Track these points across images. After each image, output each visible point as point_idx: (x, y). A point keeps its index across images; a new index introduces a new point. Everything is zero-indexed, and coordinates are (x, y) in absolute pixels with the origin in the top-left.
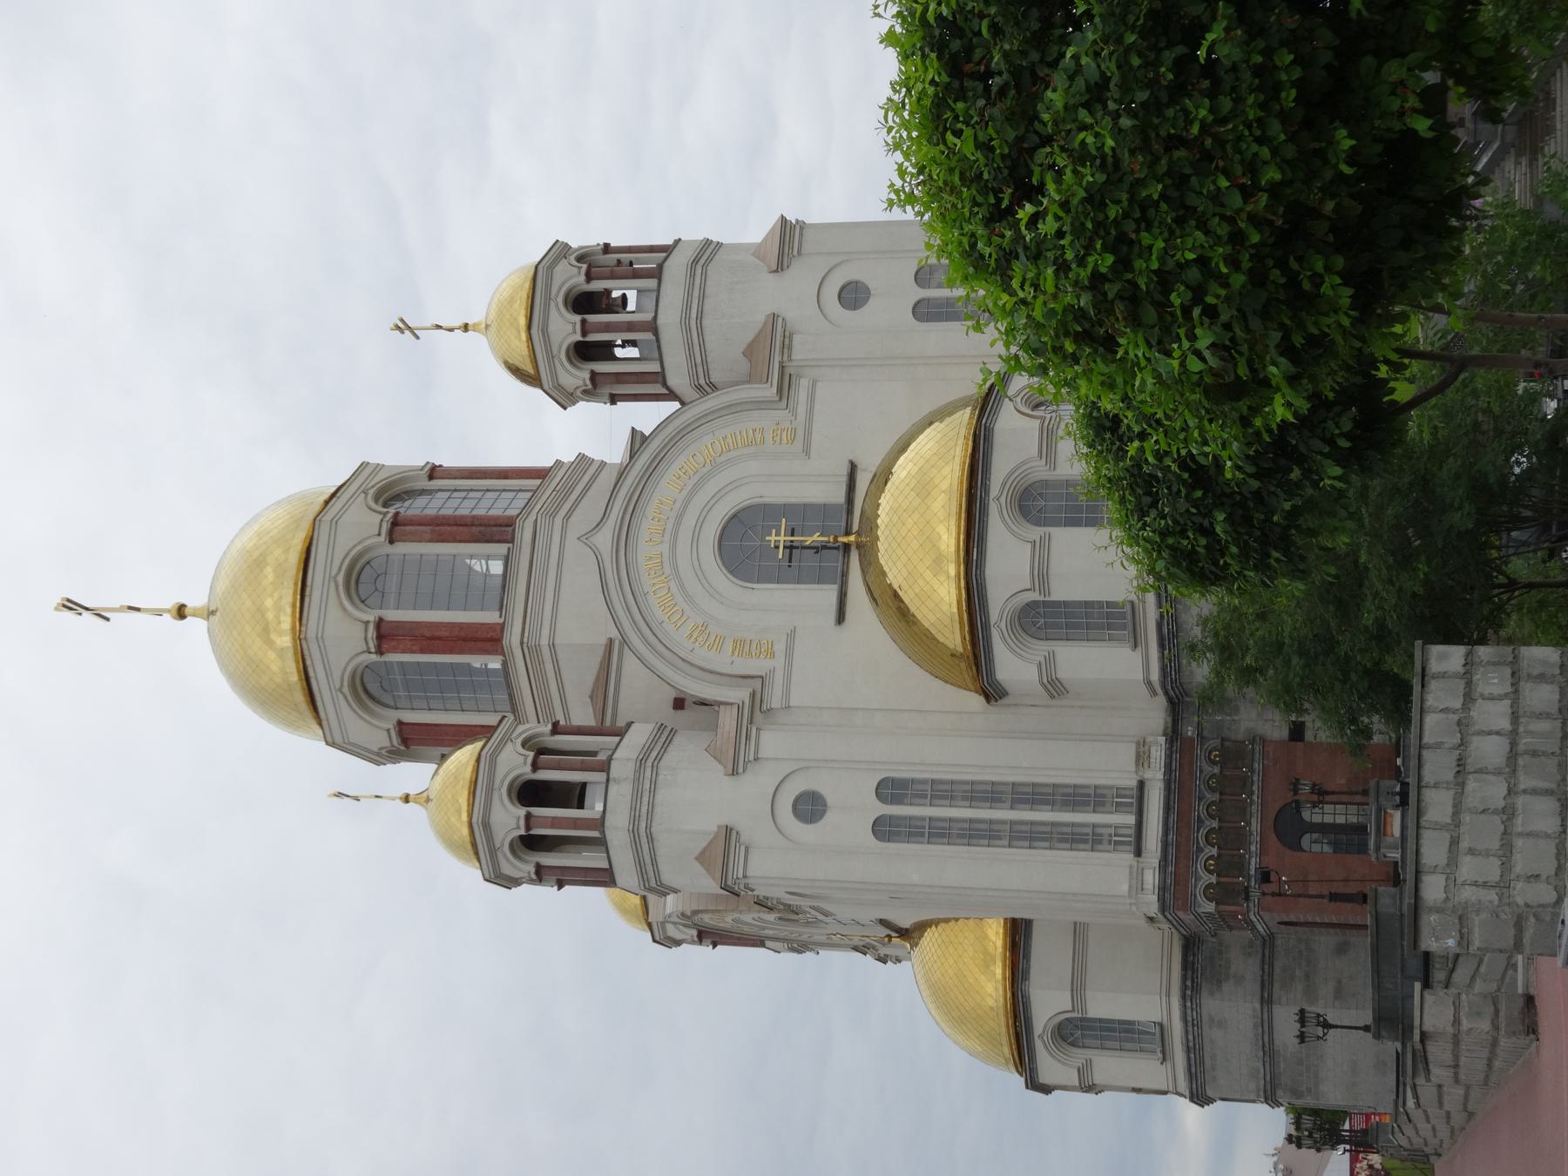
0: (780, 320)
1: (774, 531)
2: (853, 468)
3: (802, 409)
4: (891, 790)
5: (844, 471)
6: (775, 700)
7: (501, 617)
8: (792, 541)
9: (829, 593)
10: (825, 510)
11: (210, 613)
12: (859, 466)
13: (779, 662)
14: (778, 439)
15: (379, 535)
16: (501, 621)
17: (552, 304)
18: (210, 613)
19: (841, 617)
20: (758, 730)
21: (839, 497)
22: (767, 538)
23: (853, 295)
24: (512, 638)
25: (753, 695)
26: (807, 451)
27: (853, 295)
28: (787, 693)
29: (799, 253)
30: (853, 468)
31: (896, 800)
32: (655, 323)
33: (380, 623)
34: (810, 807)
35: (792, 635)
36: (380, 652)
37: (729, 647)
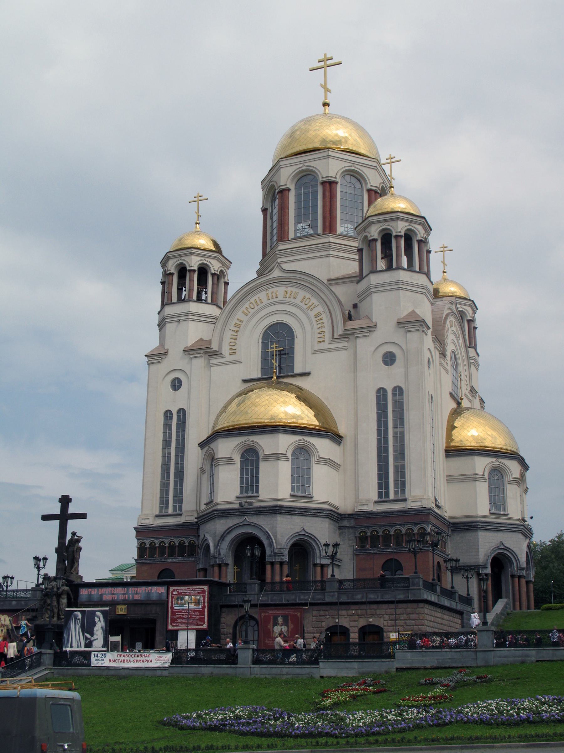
2: (307, 374)
4: (182, 413)
5: (307, 371)
6: (213, 361)
8: (276, 355)
9: (257, 374)
10: (292, 367)
15: (323, 178)
19: (245, 381)
21: (297, 370)
22: (275, 343)
25: (215, 351)
26: (316, 352)
30: (307, 374)
31: (178, 417)
33: (289, 190)
34: (176, 384)
35: (239, 362)
36: (278, 193)
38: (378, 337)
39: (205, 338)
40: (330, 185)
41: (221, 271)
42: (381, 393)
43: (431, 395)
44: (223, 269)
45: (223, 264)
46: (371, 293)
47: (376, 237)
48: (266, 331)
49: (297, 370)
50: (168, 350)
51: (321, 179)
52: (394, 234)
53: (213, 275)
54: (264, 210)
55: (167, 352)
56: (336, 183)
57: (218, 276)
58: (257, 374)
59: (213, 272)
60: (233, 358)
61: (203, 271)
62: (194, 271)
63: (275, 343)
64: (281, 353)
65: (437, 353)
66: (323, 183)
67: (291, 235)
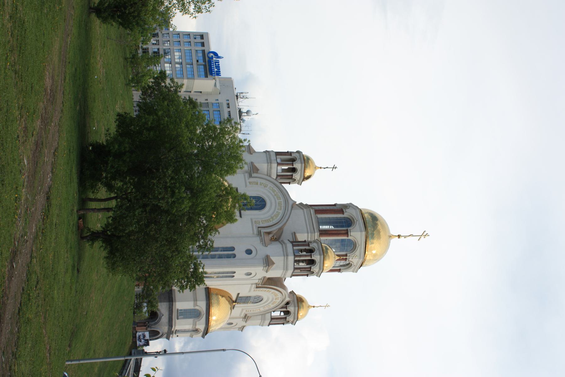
0: (264, 245)
3: (255, 228)
5: (242, 216)
6: (247, 175)
7: (317, 216)
11: (391, 237)
12: (239, 217)
13: (248, 181)
14: (259, 222)
15: (350, 230)
16: (316, 215)
17: (317, 248)
18: (391, 237)
20: (249, 170)
21: (242, 212)
23: (249, 252)
24: (312, 211)
25: (251, 175)
26: (251, 219)
27: (249, 252)
28: (244, 176)
29: (263, 259)
32: (294, 257)
33: (343, 214)
35: (246, 186)
37: (259, 184)
38: (260, 246)
39: (259, 172)
40: (347, 234)
41: (295, 180)
42: (233, 249)
43: (233, 276)
44: (297, 180)
45: (299, 181)
46: (282, 244)
47: (310, 245)
48: (261, 198)
50: (252, 154)
52: (312, 254)
53: (292, 175)
54: (335, 205)
55: (251, 154)
56: (348, 236)
57: (291, 177)
59: (294, 175)
60: (248, 184)
61: (294, 170)
62: (293, 165)
65: (257, 281)
66: (347, 230)
67: (320, 216)
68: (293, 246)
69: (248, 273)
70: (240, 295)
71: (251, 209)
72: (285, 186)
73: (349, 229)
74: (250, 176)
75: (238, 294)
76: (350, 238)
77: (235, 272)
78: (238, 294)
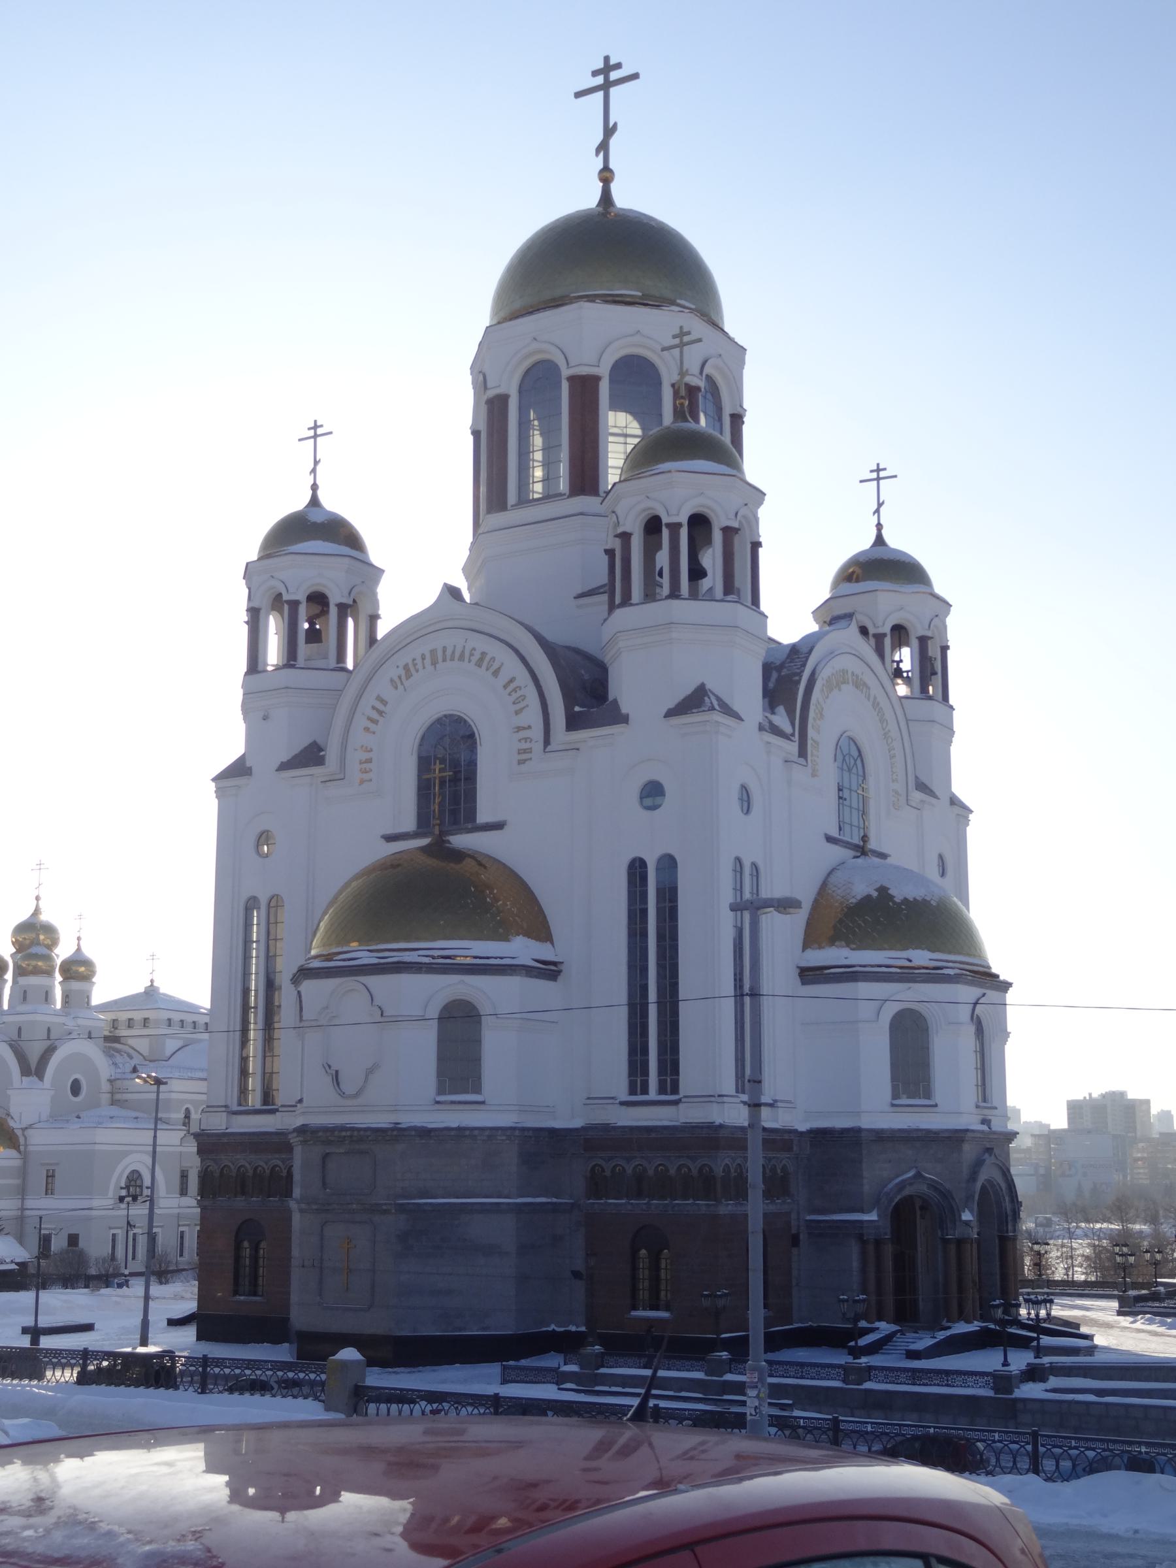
1: (443, 766)
2: (498, 826)
19: (390, 838)
22: (438, 762)
23: (652, 793)
27: (652, 793)
30: (498, 826)
42: (637, 869)
43: (755, 866)
49: (482, 817)
51: (566, 372)
56: (596, 379)
58: (409, 823)
63: (438, 762)
64: (455, 780)
68: (626, 601)
69: (741, 799)
70: (834, 833)
71: (471, 778)
72: (381, 633)
73: (566, 372)
74: (339, 777)
75: (830, 839)
76: (604, 371)
77: (738, 860)
78: (830, 839)
